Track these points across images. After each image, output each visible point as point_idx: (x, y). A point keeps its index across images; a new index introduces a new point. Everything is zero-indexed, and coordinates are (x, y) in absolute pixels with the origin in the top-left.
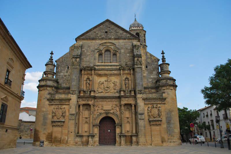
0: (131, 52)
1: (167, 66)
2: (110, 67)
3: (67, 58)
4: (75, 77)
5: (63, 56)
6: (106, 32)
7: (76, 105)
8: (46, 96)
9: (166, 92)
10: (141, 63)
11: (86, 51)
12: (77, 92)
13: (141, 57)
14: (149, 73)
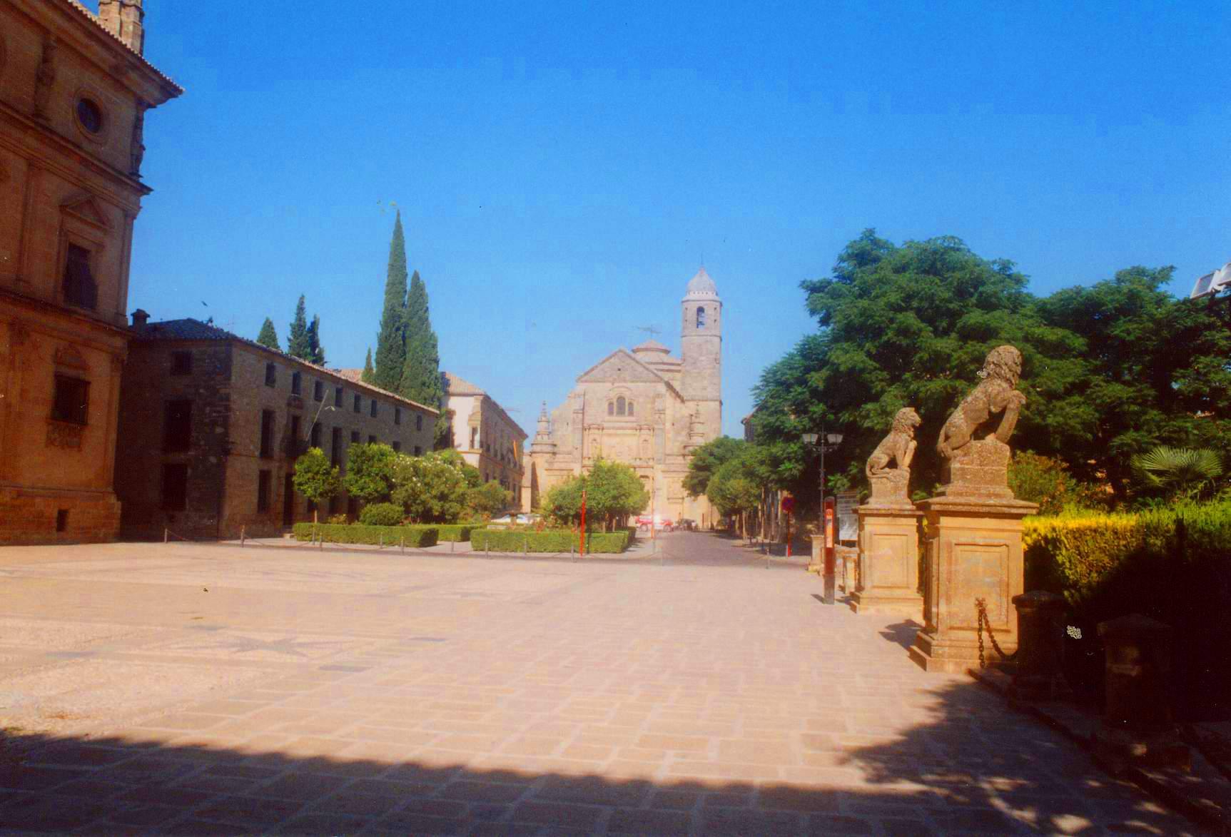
6: (619, 370)
13: (664, 414)
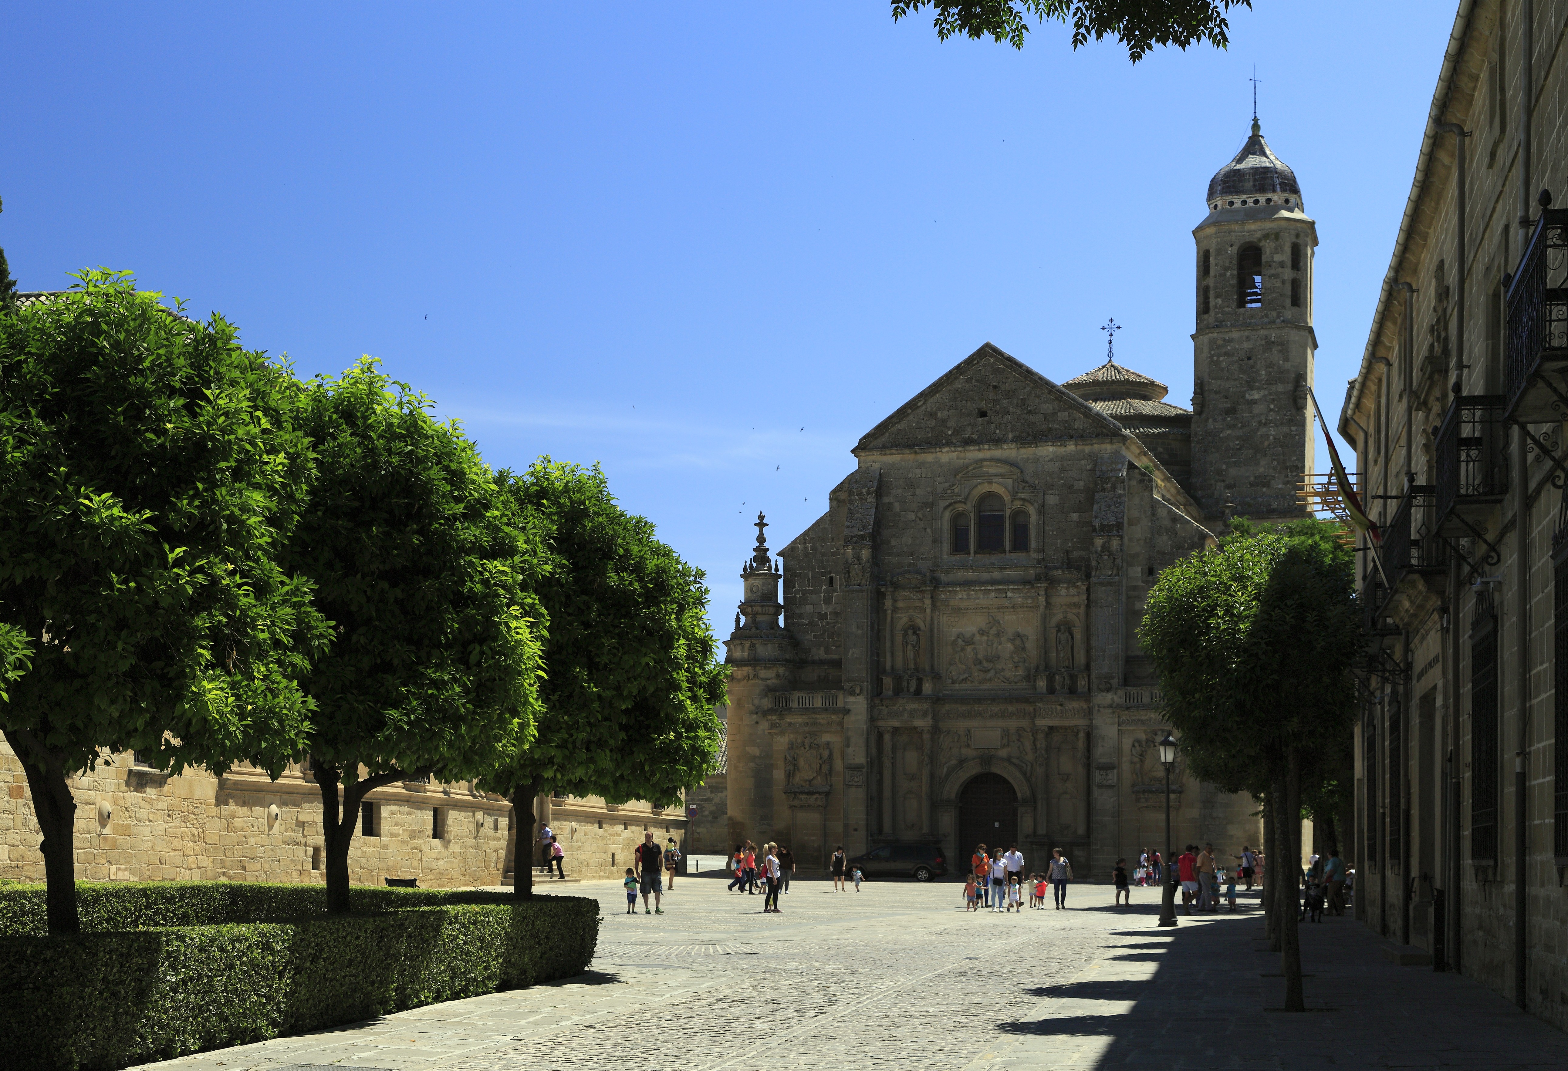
2: (996, 575)
11: (897, 506)
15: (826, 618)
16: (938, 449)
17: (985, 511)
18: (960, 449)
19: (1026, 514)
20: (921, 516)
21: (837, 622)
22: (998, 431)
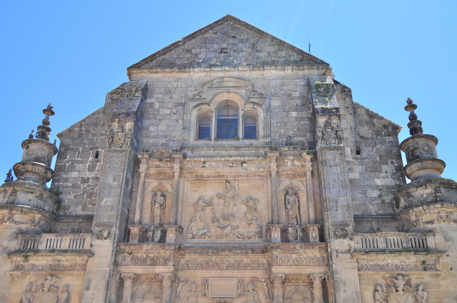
0: (303, 105)
1: (429, 143)
3: (96, 125)
4: (114, 180)
5: (84, 120)
7: (107, 275)
8: (5, 243)
9: (438, 230)
10: (340, 133)
11: (157, 105)
12: (115, 230)
14: (366, 170)
15: (88, 182)
16: (191, 69)
17: (222, 116)
18: (208, 69)
19: (255, 118)
20: (175, 112)
21: (97, 185)
22: (235, 61)
